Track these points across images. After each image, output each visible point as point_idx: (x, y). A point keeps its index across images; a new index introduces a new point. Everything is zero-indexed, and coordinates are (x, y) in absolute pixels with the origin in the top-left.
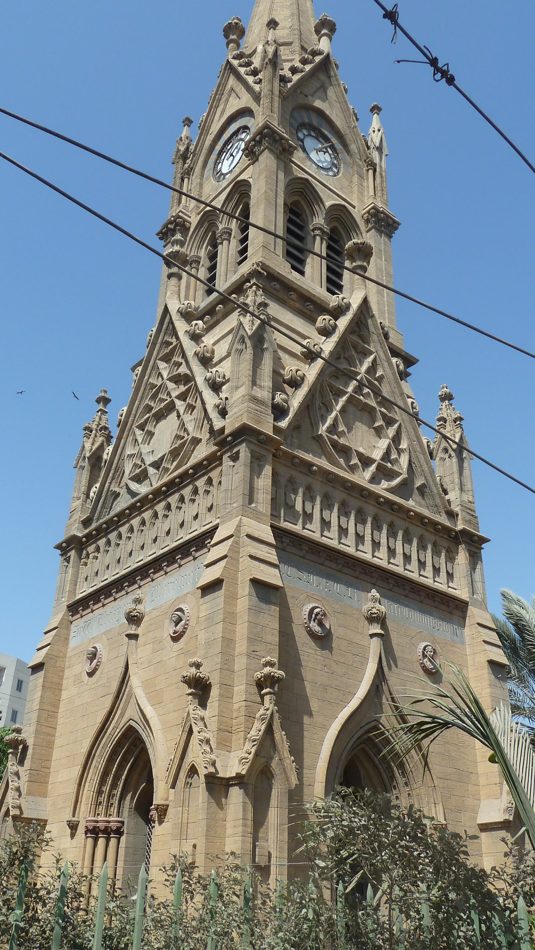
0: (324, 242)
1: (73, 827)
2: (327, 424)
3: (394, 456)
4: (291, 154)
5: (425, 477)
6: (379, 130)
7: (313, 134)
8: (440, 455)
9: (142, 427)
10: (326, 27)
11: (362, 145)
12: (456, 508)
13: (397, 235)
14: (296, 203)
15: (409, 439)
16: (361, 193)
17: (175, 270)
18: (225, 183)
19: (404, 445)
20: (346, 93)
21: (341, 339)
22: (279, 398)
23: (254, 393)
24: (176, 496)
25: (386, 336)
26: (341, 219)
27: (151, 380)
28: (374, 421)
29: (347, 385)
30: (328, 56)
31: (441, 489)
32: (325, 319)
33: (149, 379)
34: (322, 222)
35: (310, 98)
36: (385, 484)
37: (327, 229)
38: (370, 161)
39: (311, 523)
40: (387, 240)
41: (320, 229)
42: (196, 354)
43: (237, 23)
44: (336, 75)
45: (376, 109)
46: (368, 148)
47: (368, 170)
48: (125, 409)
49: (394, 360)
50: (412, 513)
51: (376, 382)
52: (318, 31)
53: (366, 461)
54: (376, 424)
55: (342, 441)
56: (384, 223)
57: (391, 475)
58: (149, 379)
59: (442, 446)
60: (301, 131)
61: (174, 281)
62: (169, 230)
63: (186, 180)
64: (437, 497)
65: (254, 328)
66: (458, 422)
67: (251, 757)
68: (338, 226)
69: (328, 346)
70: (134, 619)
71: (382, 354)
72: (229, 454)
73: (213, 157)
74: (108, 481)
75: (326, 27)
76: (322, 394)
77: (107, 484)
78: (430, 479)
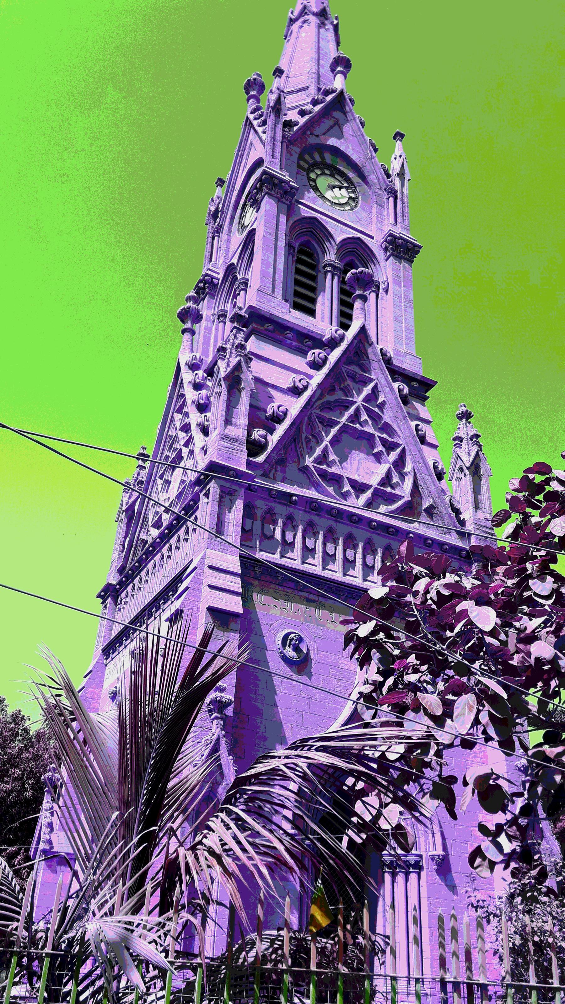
0: (336, 278)
2: (315, 455)
3: (395, 479)
4: (293, 195)
5: (433, 498)
6: (400, 156)
7: (327, 172)
8: (457, 474)
9: (161, 477)
10: (342, 64)
11: (381, 174)
12: (470, 527)
13: (418, 259)
14: (307, 244)
15: (413, 462)
16: (380, 221)
17: (188, 325)
19: (408, 468)
20: (363, 127)
21: (331, 371)
22: (257, 434)
23: (227, 431)
24: (175, 537)
25: (388, 361)
26: (356, 252)
27: (170, 433)
28: (373, 447)
29: (342, 415)
30: (342, 92)
31: (450, 509)
32: (314, 353)
33: (168, 431)
34: (333, 257)
35: (322, 137)
36: (383, 508)
37: (338, 264)
38: (390, 188)
39: (292, 552)
40: (407, 265)
41: (330, 265)
42: (193, 402)
43: (255, 79)
44: (351, 110)
45: (399, 136)
46: (389, 176)
47: (388, 199)
49: (396, 385)
50: (411, 535)
51: (376, 410)
52: (333, 70)
53: (359, 488)
54: (376, 451)
55: (333, 470)
56: (403, 250)
57: (391, 499)
58: (168, 431)
59: (458, 466)
60: (313, 171)
61: (187, 335)
62: (200, 288)
63: (216, 238)
64: (446, 517)
65: (229, 369)
66: (474, 440)
69: (318, 377)
71: (383, 381)
72: (204, 492)
73: (239, 211)
74: (138, 530)
75: (342, 64)
76: (311, 426)
77: (137, 533)
78: (438, 500)
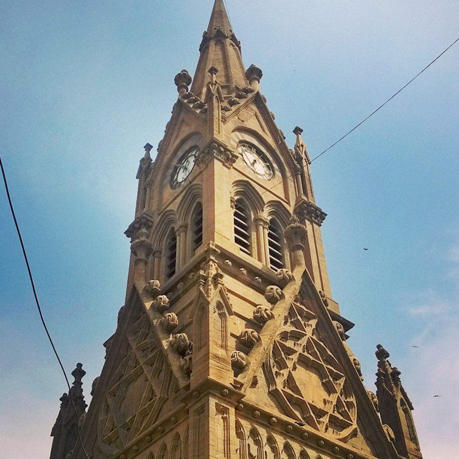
4: (234, 162)
18: (179, 190)
31: (388, 438)
32: (272, 289)
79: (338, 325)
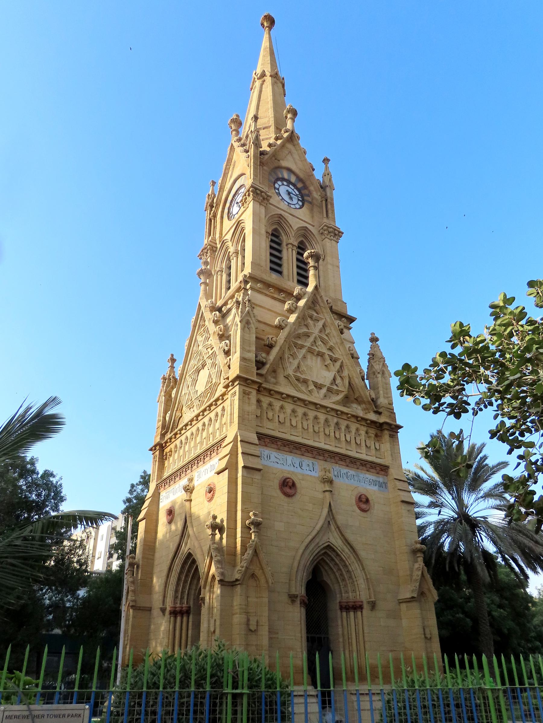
0: (294, 252)
1: (163, 610)
3: (338, 381)
4: (268, 200)
14: (276, 230)
19: (345, 373)
25: (331, 308)
48: (181, 366)
49: (337, 322)
53: (319, 387)
67: (243, 569)
68: (304, 240)
70: (189, 490)
79: (339, 324)
